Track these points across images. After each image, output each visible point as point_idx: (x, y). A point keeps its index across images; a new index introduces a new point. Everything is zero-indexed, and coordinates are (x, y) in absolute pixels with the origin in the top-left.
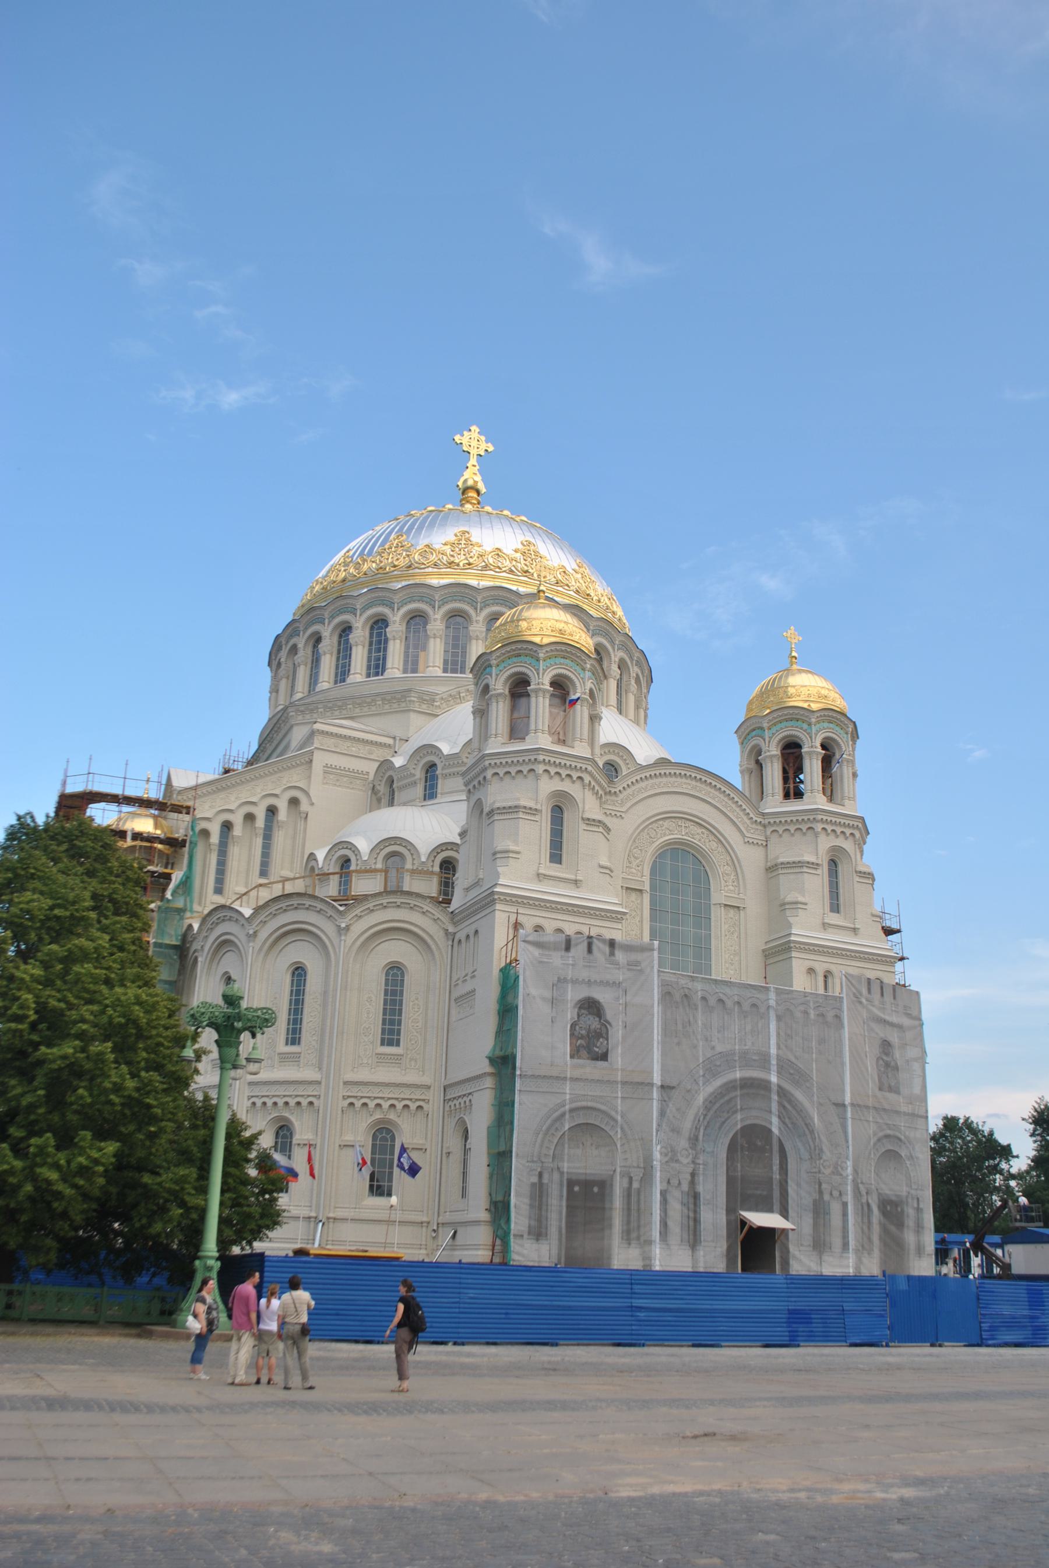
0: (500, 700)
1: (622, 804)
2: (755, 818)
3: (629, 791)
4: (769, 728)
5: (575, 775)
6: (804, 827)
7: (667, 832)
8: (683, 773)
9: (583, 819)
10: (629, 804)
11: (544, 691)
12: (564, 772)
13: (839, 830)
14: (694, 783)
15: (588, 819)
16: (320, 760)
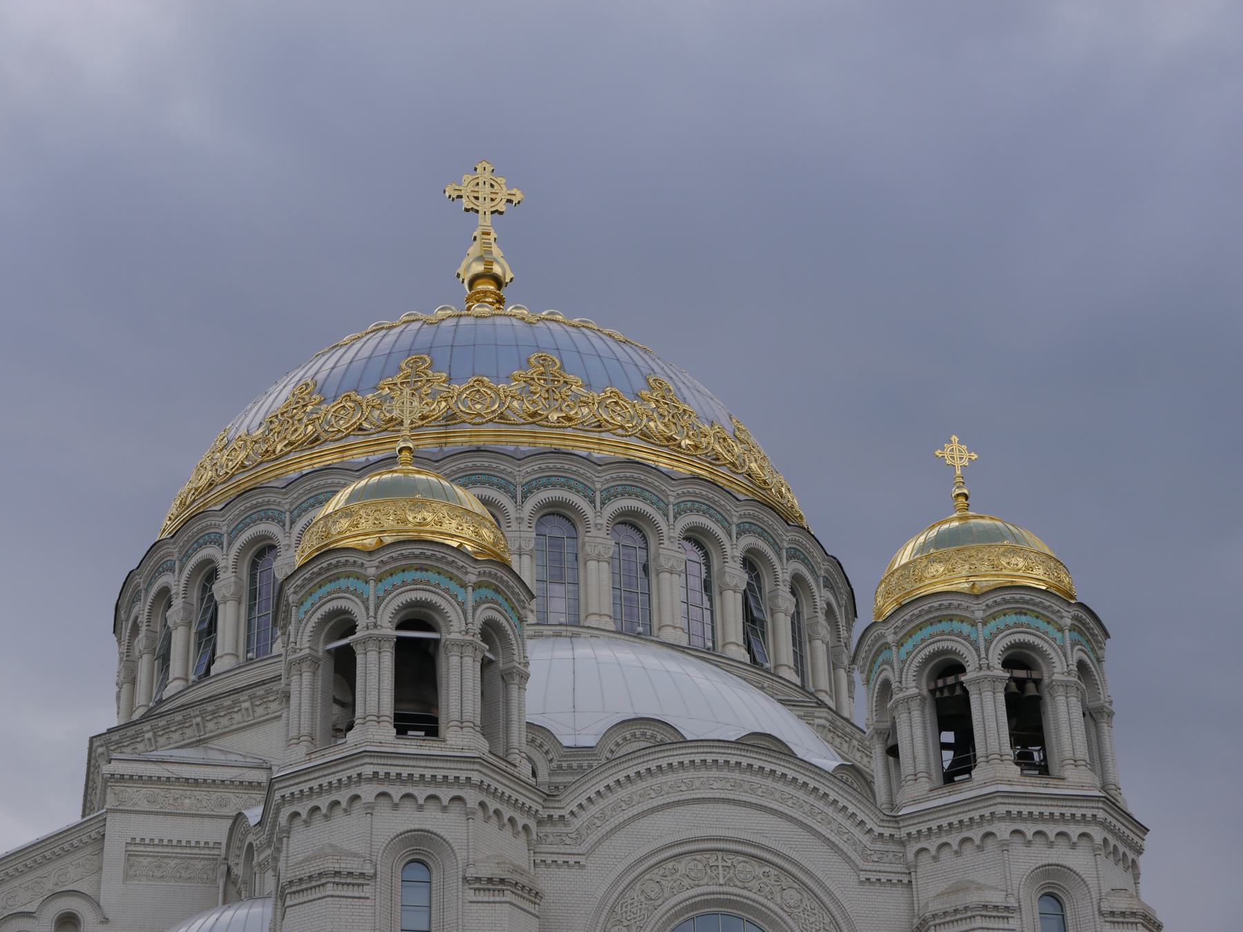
0: (305, 667)
1: (579, 837)
2: (877, 830)
3: (593, 810)
4: (900, 644)
5: (445, 794)
6: (976, 834)
7: (686, 882)
8: (709, 758)
9: (464, 879)
10: (594, 837)
11: (379, 640)
12: (421, 793)
13: (1051, 830)
14: (736, 775)
15: (478, 879)
16: (119, 831)
